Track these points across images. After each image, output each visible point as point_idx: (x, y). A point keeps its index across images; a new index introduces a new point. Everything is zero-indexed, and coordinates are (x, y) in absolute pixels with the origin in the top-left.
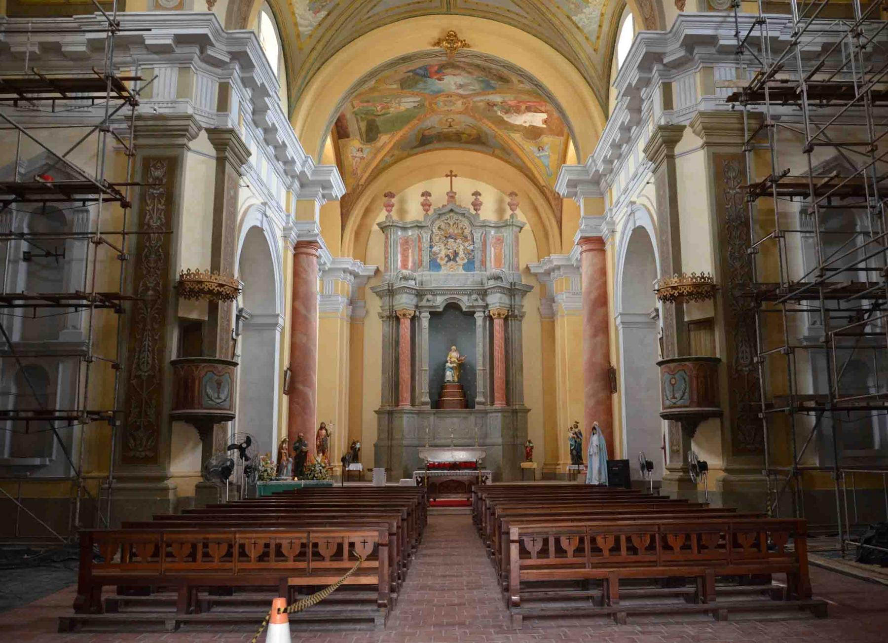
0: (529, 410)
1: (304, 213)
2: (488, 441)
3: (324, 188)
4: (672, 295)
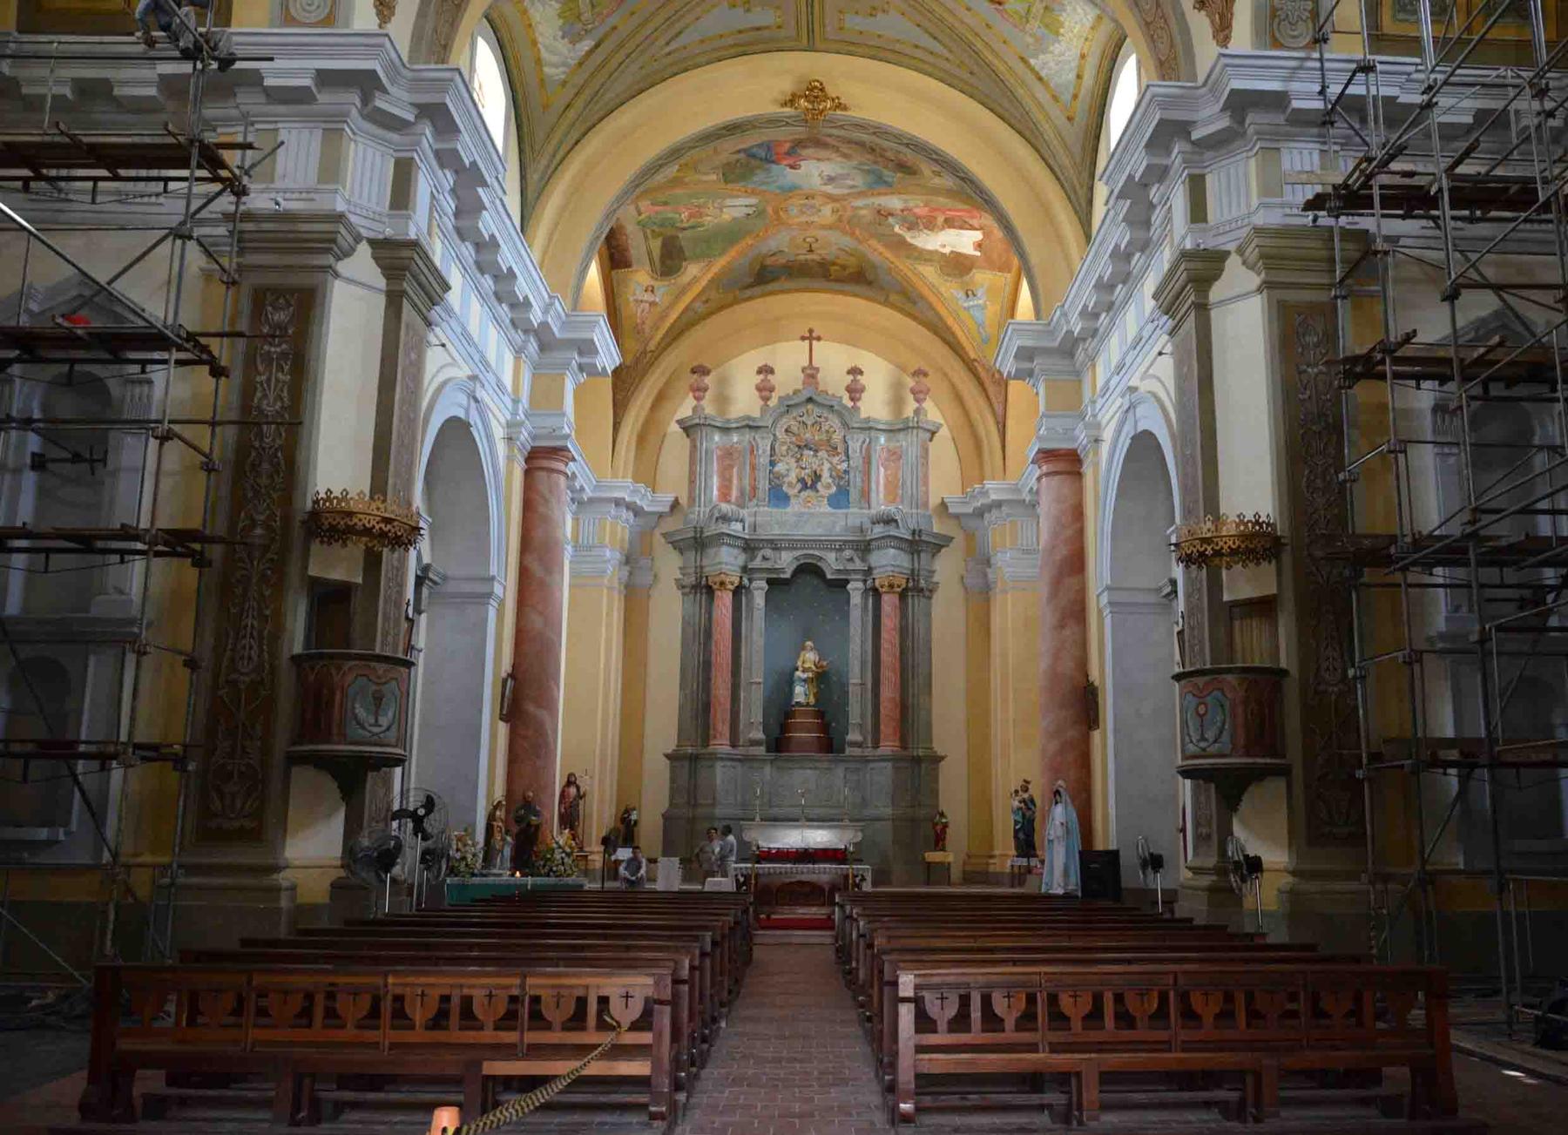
0: (942, 758)
1: (545, 397)
3: (581, 354)
4: (1202, 554)
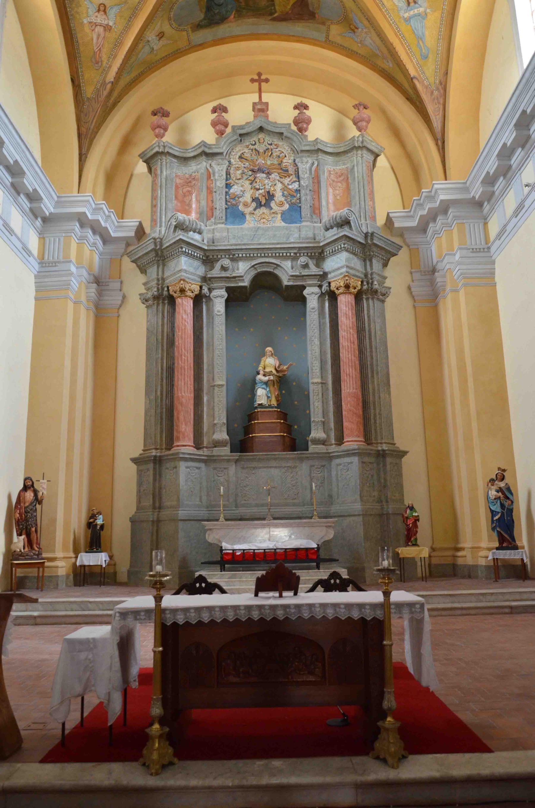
0: (405, 453)
2: (335, 509)
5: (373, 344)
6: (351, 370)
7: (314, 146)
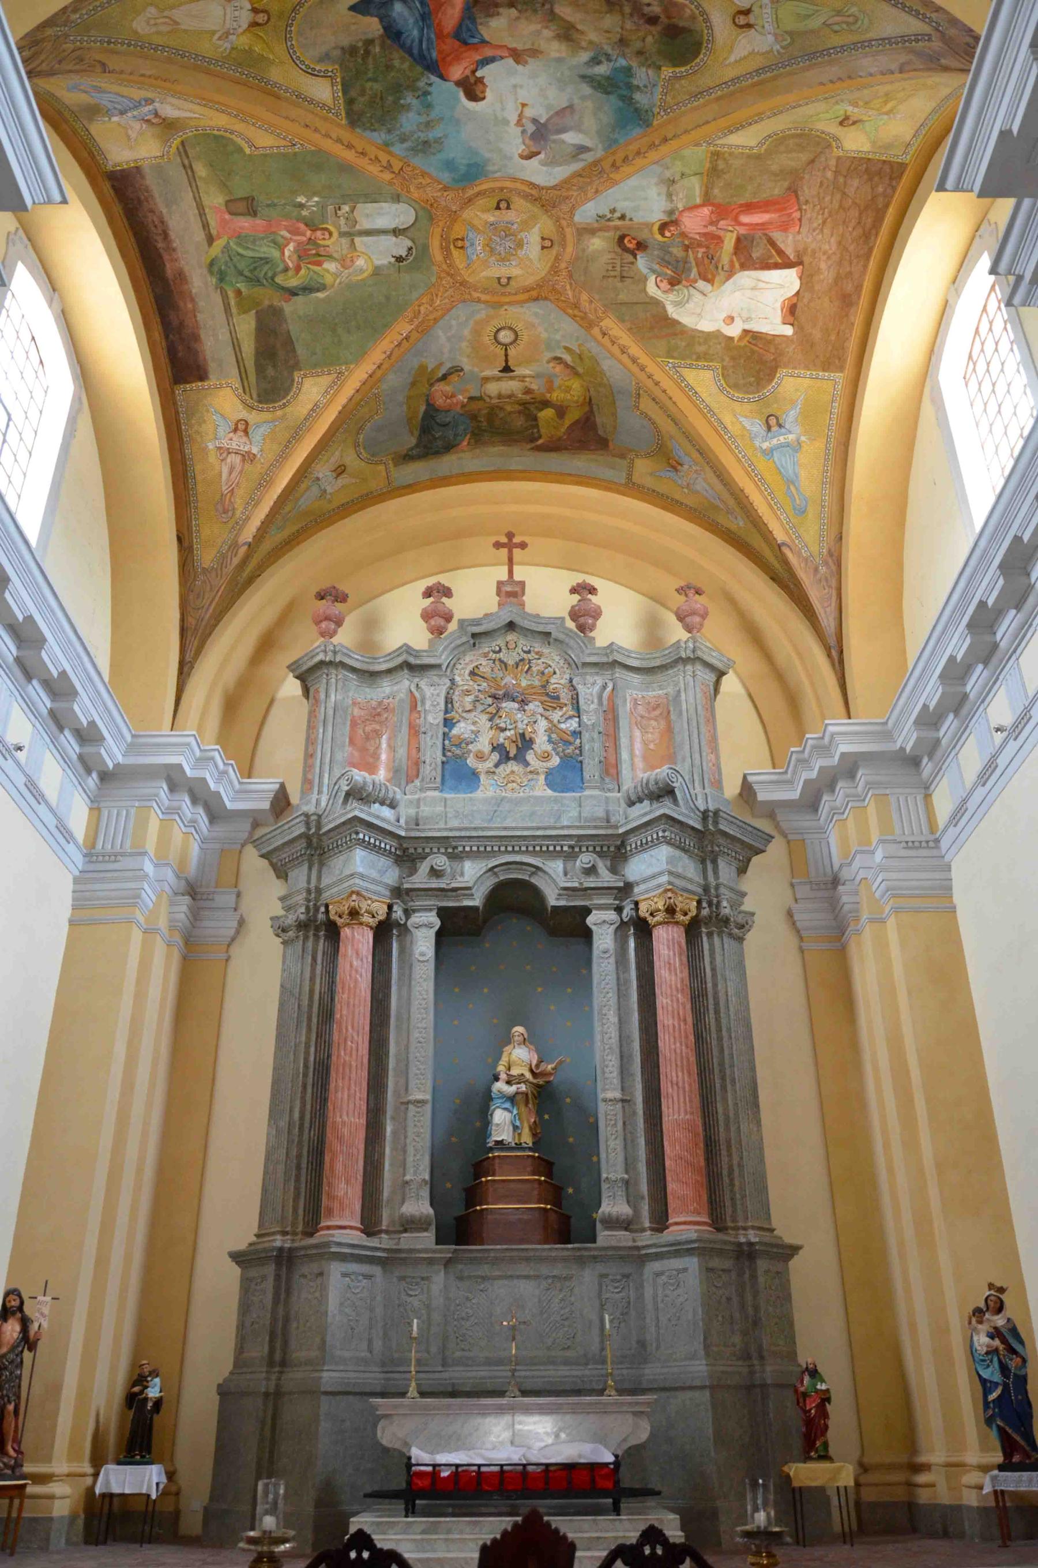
0: (795, 1249)
2: (651, 1372)
5: (724, 1022)
6: (680, 1074)
7: (607, 655)
